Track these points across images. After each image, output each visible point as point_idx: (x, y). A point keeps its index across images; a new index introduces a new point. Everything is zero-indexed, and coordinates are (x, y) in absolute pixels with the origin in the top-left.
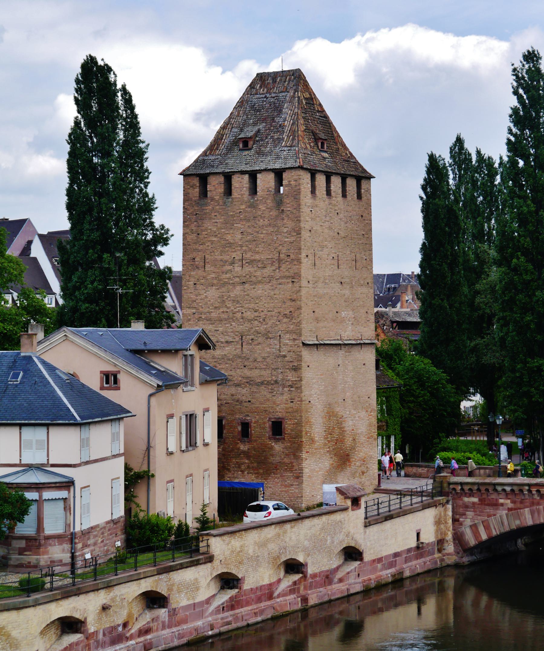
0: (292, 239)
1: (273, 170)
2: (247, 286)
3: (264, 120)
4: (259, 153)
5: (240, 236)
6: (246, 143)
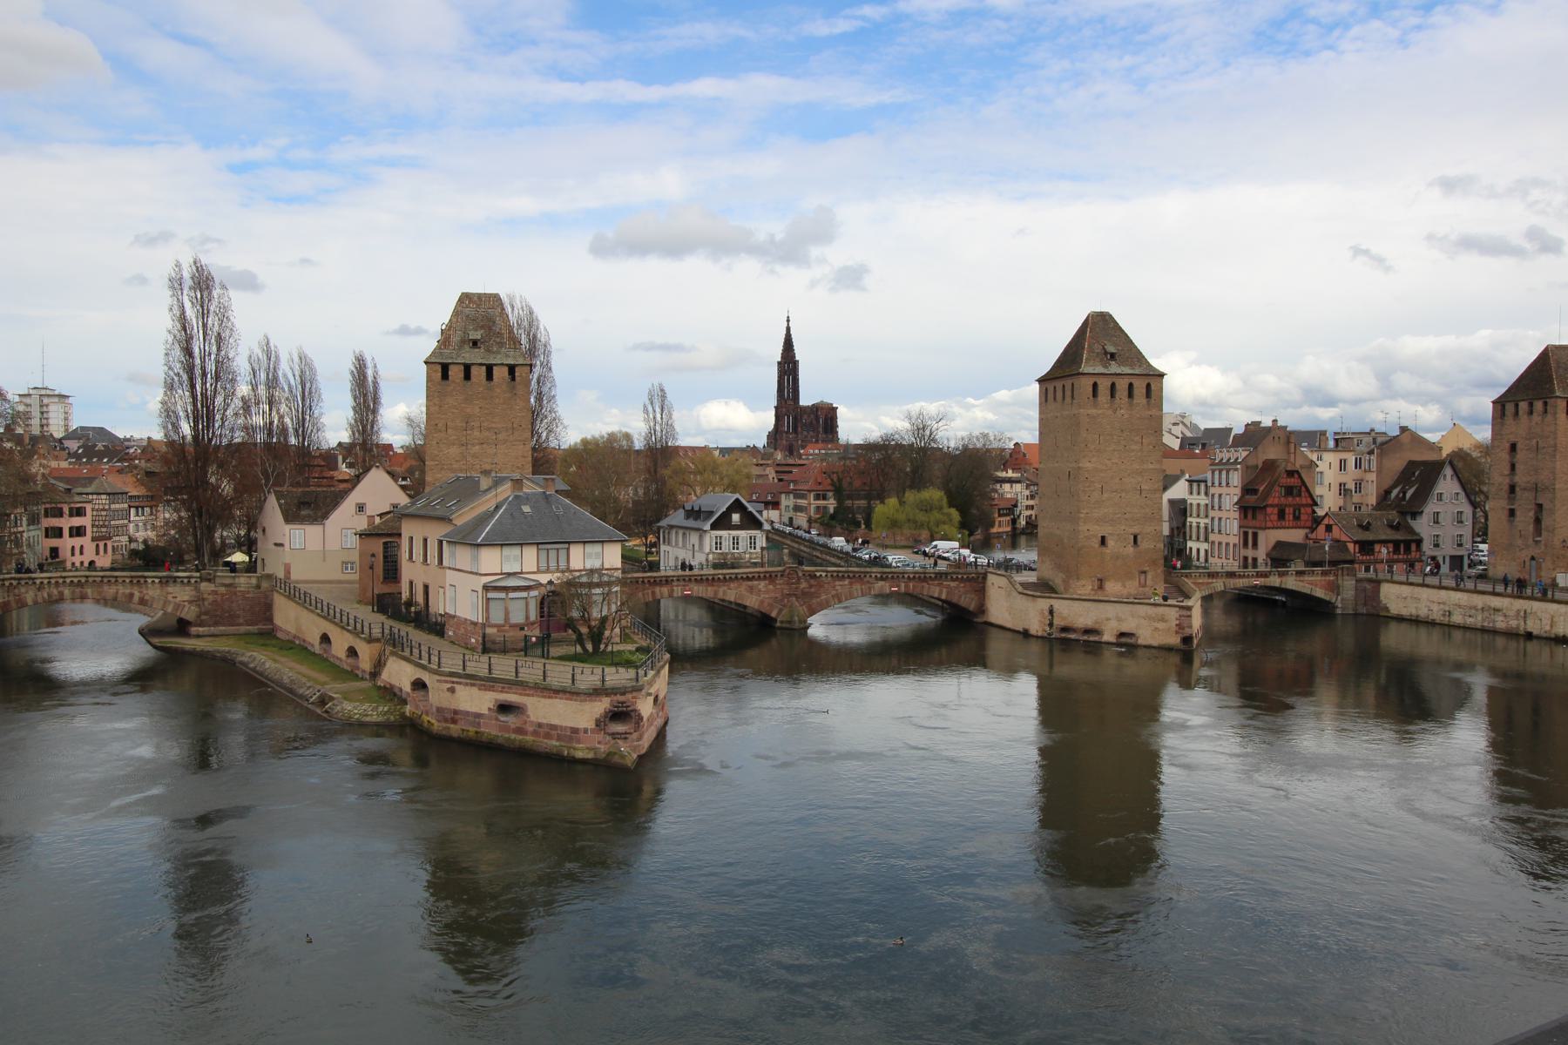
0: (524, 414)
1: (507, 365)
2: (484, 446)
3: (482, 327)
4: (488, 351)
5: (478, 410)
6: (475, 343)
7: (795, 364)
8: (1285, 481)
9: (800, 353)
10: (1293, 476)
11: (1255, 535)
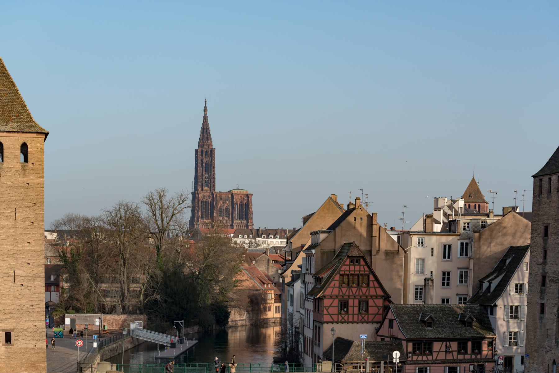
7: (212, 151)
8: (347, 268)
9: (216, 142)
10: (358, 262)
11: (319, 328)
